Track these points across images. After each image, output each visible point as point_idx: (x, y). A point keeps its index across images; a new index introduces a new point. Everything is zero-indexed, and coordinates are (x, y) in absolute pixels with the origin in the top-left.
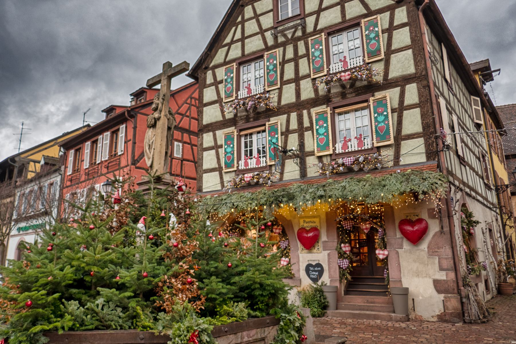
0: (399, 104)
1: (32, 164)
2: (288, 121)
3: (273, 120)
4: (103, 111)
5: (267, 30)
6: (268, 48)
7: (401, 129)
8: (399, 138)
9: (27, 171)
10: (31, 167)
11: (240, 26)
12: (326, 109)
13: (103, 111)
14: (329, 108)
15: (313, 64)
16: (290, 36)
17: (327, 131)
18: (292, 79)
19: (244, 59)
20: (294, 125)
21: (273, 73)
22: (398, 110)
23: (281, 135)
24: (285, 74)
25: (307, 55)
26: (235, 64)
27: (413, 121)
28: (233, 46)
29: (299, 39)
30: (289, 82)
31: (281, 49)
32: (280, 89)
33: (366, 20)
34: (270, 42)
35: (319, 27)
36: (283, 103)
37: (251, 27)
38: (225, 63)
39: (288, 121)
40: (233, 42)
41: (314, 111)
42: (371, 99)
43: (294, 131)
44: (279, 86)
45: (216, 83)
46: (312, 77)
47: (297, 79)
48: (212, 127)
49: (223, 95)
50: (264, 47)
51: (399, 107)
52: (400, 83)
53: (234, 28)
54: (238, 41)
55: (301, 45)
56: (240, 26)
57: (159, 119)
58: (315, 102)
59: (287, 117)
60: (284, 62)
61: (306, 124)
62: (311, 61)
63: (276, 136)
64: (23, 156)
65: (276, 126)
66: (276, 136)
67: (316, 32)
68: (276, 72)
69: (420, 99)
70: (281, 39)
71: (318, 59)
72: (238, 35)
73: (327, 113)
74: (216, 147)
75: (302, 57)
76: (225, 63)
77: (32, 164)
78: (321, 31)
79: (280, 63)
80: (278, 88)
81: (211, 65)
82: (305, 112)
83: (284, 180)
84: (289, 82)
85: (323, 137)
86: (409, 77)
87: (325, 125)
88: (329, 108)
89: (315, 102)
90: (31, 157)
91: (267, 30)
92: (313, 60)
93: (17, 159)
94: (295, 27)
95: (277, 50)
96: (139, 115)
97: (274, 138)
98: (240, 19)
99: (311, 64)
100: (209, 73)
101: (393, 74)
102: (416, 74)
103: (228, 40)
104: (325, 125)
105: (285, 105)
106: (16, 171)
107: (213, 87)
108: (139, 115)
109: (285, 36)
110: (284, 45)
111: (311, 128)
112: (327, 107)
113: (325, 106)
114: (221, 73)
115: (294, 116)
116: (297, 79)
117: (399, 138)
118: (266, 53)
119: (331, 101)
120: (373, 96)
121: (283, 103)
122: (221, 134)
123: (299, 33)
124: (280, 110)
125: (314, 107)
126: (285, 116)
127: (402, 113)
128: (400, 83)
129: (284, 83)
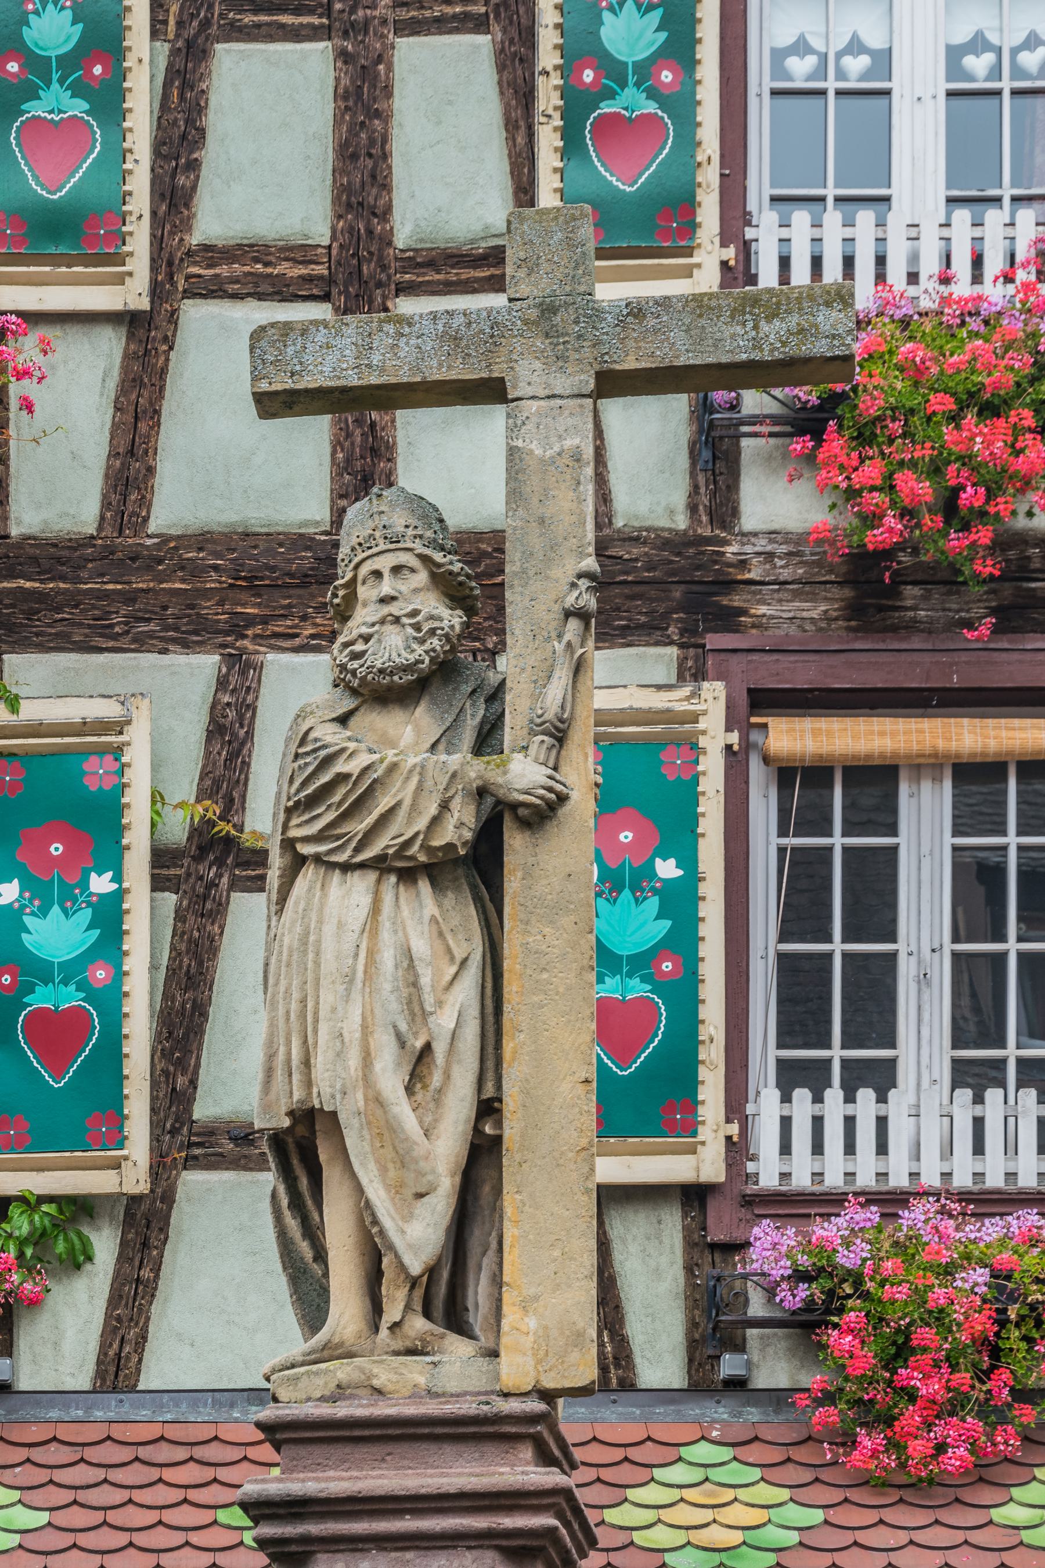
2: (229, 735)
12: (675, 700)
14: (714, 695)
15: (571, 144)
17: (682, 942)
18: (299, 252)
21: (78, 108)
23: (158, 884)
24: (214, 156)
32: (147, 337)
44: (134, 293)
57: (542, 814)
59: (222, 683)
62: (548, 96)
63: (101, 884)
65: (101, 767)
66: (101, 884)
68: (109, 104)
71: (632, 102)
73: (693, 748)
80: (130, 321)
83: (141, 1387)
85: (637, 989)
87: (667, 869)
88: (714, 695)
92: (576, 105)
97: (69, 906)
99: (548, 140)
104: (667, 869)
105: (203, 540)
112: (693, 672)
119: (729, 620)
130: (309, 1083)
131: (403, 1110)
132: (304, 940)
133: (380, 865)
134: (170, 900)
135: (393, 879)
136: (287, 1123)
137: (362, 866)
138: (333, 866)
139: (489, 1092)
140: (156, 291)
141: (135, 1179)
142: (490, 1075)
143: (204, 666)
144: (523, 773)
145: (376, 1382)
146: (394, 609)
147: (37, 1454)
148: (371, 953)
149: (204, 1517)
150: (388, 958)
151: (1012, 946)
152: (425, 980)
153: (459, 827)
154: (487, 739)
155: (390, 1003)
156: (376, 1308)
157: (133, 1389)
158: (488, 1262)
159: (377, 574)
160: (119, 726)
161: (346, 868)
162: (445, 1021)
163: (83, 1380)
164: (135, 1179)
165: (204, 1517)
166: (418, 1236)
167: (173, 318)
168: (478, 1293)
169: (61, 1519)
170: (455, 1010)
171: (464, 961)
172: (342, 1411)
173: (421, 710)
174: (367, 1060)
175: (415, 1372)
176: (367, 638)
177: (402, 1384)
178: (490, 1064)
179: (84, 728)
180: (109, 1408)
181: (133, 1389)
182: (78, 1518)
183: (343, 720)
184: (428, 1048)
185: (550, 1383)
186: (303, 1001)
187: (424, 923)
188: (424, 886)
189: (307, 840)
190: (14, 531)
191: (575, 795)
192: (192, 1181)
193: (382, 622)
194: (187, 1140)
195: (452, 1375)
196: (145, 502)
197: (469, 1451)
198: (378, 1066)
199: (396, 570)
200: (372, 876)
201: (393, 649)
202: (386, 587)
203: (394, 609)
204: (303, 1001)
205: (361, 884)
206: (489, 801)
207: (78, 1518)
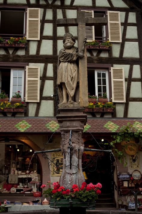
0: (129, 76)
2: (45, 69)
3: (32, 65)
7: (130, 93)
8: (129, 99)
20: (50, 73)
22: (128, 80)
23: (40, 79)
33: (111, 12)
39: (45, 69)
42: (112, 68)
51: (128, 78)
52: (130, 62)
79: (41, 20)
86: (135, 60)
101: (125, 55)
105: (44, 55)
115: (50, 66)
118: (28, 9)
124: (38, 58)
127: (131, 83)
128: (130, 62)
129: (43, 37)
130: (62, 80)
131: (71, 82)
132: (61, 68)
133: (68, 62)
134: (41, 80)
135: (69, 63)
136: (60, 84)
137: (67, 62)
138: (64, 62)
139: (78, 81)
140: (40, 39)
141: (38, 101)
142: (78, 79)
143: (43, 65)
144: (81, 54)
145: (69, 106)
146: (69, 41)
147: (31, 121)
148: (68, 69)
149: (44, 126)
150: (69, 69)
151: (102, 86)
152: (72, 71)
153: (75, 59)
154: (77, 52)
155: (70, 73)
156: (68, 101)
157: (38, 116)
158: (78, 95)
159: (67, 39)
160: (38, 69)
161: (65, 62)
162: (74, 75)
163: (34, 116)
164: (38, 101)
165: (44, 126)
166: (72, 93)
167: (41, 41)
168: (77, 99)
169: (33, 126)
170: (75, 74)
171: (76, 70)
172: (66, 108)
173: (71, 50)
174: (67, 78)
175: (72, 105)
176: (66, 44)
177: (71, 106)
178: (78, 79)
179: (35, 69)
180: (36, 118)
181: (38, 116)
182: (34, 126)
183: (64, 50)
184: (73, 77)
185: (84, 106)
186: (61, 73)
187: (72, 67)
188: (72, 64)
189: (61, 60)
190: (30, 55)
191: (85, 56)
192: (43, 101)
193: (68, 42)
194: (42, 98)
195: (76, 105)
196: (39, 53)
197: (77, 112)
198: (69, 79)
199: (69, 38)
200: (67, 63)
201: (69, 44)
202: (68, 40)
203: (69, 41)
204: (61, 73)
205: (66, 63)
206: (78, 57)
207: (34, 126)
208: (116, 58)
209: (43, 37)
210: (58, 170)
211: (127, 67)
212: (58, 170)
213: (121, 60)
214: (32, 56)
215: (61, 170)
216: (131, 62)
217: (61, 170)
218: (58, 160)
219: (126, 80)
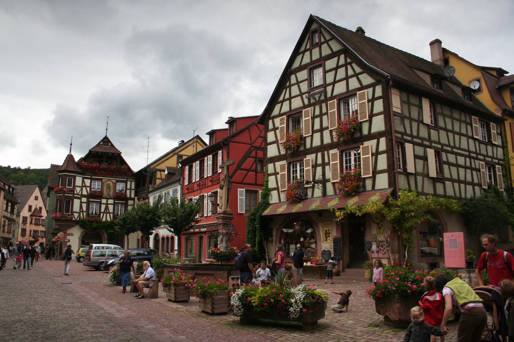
1: (158, 172)
4: (207, 134)
5: (304, 93)
6: (305, 107)
8: (375, 172)
9: (156, 178)
10: (158, 175)
11: (288, 89)
13: (207, 134)
16: (317, 99)
19: (292, 113)
20: (319, 161)
25: (327, 113)
26: (285, 116)
27: (383, 162)
28: (284, 103)
29: (323, 101)
30: (317, 131)
31: (312, 108)
32: (312, 136)
34: (306, 102)
35: (334, 94)
36: (314, 145)
37: (295, 91)
38: (280, 115)
40: (284, 100)
41: (332, 152)
43: (319, 165)
45: (275, 129)
46: (330, 129)
47: (321, 130)
48: (274, 160)
49: (279, 138)
50: (302, 105)
53: (285, 90)
54: (287, 100)
55: (324, 105)
56: (288, 89)
58: (331, 146)
60: (313, 118)
61: (326, 161)
64: (152, 167)
67: (332, 98)
69: (387, 147)
70: (312, 101)
72: (287, 96)
74: (276, 174)
75: (324, 114)
76: (280, 115)
77: (158, 172)
78: (335, 97)
81: (272, 116)
82: (326, 152)
84: (317, 131)
89: (331, 146)
90: (158, 167)
91: (304, 93)
93: (148, 170)
94: (320, 93)
95: (309, 108)
96: (231, 143)
98: (288, 84)
100: (270, 122)
101: (373, 131)
102: (385, 131)
103: (281, 99)
106: (148, 179)
107: (273, 132)
108: (231, 143)
109: (315, 98)
110: (314, 105)
111: (328, 164)
113: (336, 149)
114: (277, 121)
115: (319, 154)
116: (321, 130)
117: (375, 172)
118: (303, 110)
120: (363, 144)
121: (314, 145)
122: (278, 164)
123: (323, 98)
125: (331, 149)
126: (314, 155)
129: (314, 132)
208: (365, 136)
209: (314, 132)
210: (326, 238)
211: (375, 141)
212: (326, 238)
213: (371, 137)
214: (308, 149)
215: (328, 238)
216: (378, 136)
217: (328, 238)
218: (326, 231)
219: (373, 155)
